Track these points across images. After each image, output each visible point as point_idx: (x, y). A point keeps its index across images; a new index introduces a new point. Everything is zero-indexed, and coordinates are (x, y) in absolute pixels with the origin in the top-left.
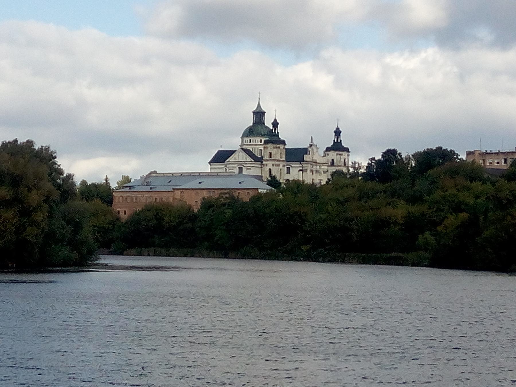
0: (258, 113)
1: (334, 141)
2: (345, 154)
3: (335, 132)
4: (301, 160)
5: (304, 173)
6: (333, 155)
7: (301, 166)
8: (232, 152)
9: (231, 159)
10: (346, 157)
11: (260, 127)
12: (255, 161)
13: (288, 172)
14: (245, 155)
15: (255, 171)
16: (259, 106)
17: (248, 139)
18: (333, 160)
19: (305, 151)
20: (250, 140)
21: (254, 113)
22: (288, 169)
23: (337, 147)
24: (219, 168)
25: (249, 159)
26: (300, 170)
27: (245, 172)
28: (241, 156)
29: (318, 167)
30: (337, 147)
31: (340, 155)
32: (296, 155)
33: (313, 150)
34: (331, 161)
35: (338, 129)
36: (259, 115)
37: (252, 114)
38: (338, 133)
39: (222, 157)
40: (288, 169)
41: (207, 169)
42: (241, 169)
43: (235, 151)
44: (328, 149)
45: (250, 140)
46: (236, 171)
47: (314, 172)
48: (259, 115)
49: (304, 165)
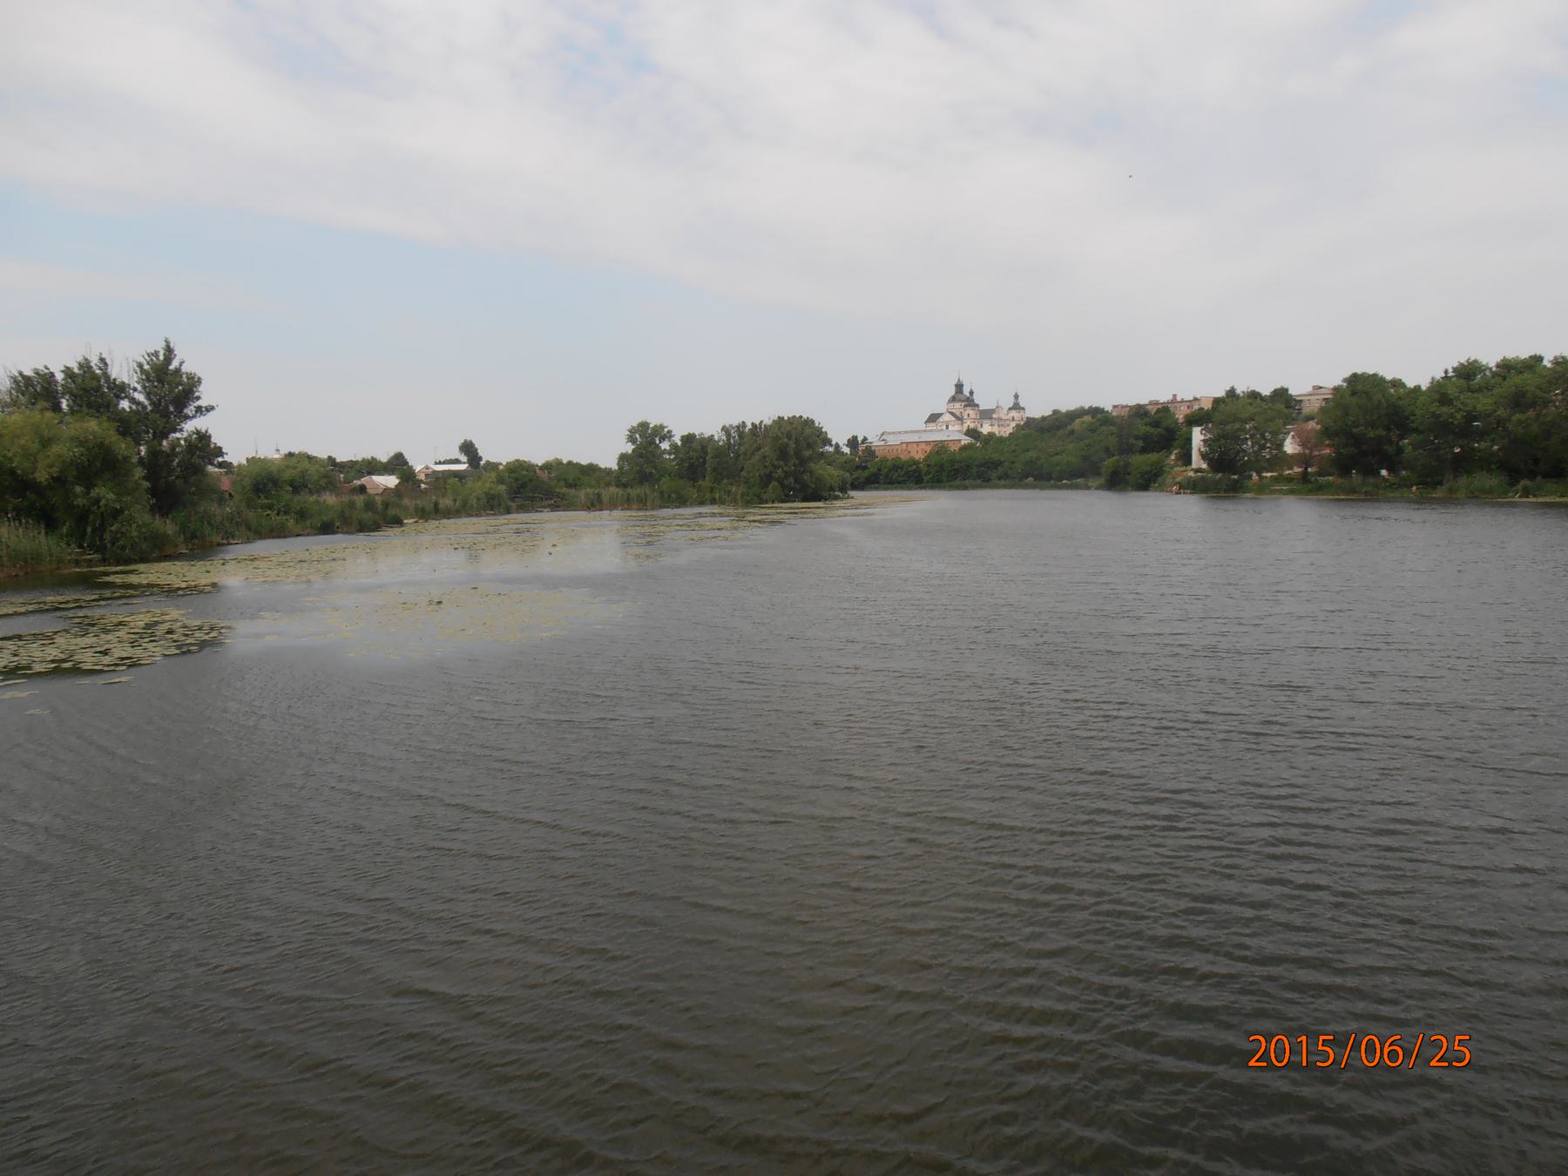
6: (1014, 413)
8: (940, 415)
11: (962, 396)
15: (957, 427)
19: (993, 411)
23: (1016, 407)
24: (932, 426)
28: (947, 417)
30: (1016, 407)
32: (987, 415)
36: (959, 387)
38: (1016, 397)
39: (933, 418)
41: (923, 427)
48: (959, 387)
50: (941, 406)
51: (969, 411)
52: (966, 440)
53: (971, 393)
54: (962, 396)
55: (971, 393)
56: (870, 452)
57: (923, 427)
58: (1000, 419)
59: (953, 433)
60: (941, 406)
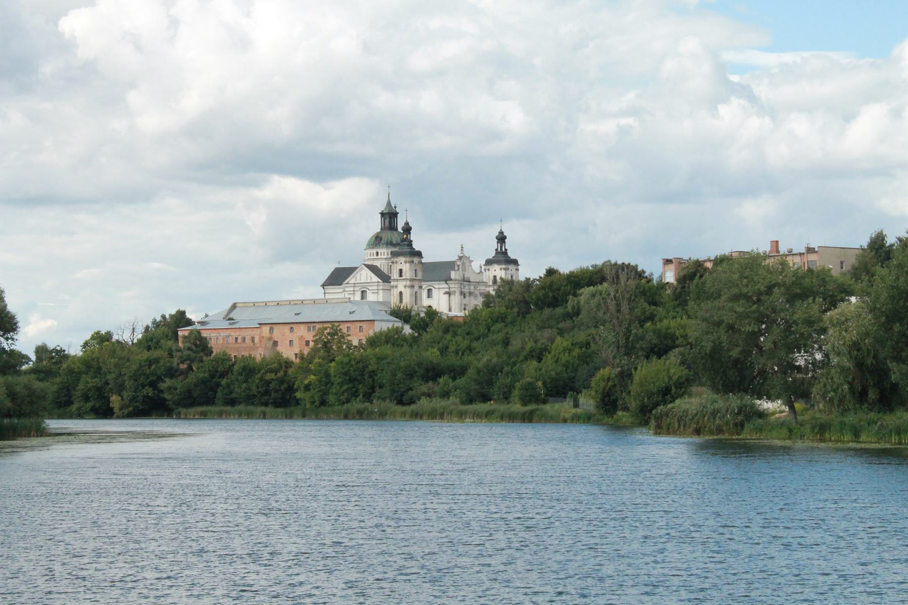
0: (389, 213)
1: (497, 250)
2: (512, 267)
3: (497, 238)
4: (448, 279)
5: (452, 297)
6: (498, 271)
7: (446, 286)
9: (351, 280)
10: (514, 272)
12: (384, 282)
13: (429, 295)
16: (389, 204)
17: (374, 251)
18: (495, 277)
19: (451, 265)
20: (377, 253)
21: (382, 214)
22: (429, 291)
23: (503, 258)
24: (335, 293)
25: (375, 279)
26: (446, 293)
27: (371, 297)
28: (364, 276)
29: (472, 287)
31: (505, 269)
33: (464, 264)
34: (492, 278)
35: (501, 233)
37: (380, 216)
38: (501, 239)
39: (339, 277)
40: (429, 291)
41: (317, 292)
42: (363, 293)
43: (356, 268)
44: (489, 262)
45: (377, 253)
46: (358, 297)
47: (467, 295)
49: (451, 286)
51: (403, 264)
52: (387, 324)
54: (394, 234)
55: (407, 229)
56: (200, 344)
57: (317, 292)
58: (465, 281)
59: (367, 307)
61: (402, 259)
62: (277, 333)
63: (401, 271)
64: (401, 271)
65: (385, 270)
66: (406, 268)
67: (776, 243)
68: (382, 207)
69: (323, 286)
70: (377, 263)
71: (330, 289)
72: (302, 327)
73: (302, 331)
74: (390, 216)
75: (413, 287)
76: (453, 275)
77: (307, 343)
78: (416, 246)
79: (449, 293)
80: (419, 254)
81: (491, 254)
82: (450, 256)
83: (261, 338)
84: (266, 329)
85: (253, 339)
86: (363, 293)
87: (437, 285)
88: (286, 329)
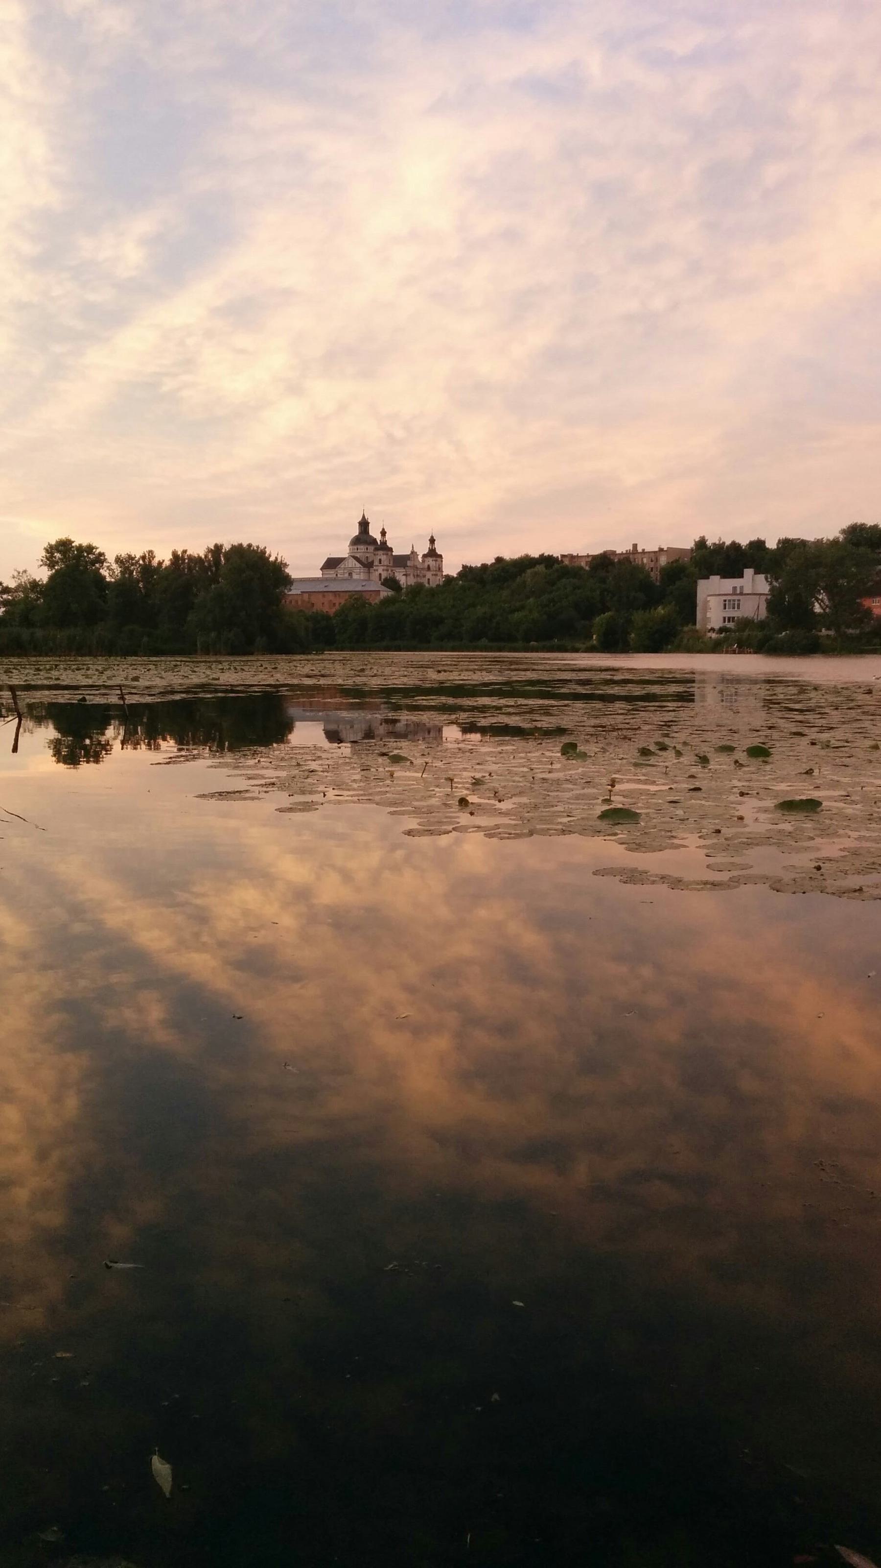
2: (439, 559)
4: (405, 566)
6: (430, 561)
9: (342, 566)
14: (355, 562)
16: (364, 517)
21: (360, 523)
23: (432, 553)
24: (331, 573)
25: (358, 565)
27: (355, 576)
28: (353, 563)
30: (432, 553)
32: (401, 561)
35: (432, 537)
38: (432, 541)
39: (332, 564)
41: (319, 574)
44: (424, 556)
46: (347, 575)
48: (364, 524)
50: (342, 550)
52: (386, 593)
53: (383, 533)
55: (383, 533)
58: (415, 567)
60: (342, 550)
61: (381, 552)
62: (313, 599)
63: (380, 560)
64: (380, 560)
65: (363, 560)
66: (383, 558)
67: (635, 546)
68: (360, 519)
69: (321, 569)
70: (358, 555)
71: (326, 571)
72: (330, 594)
73: (331, 597)
74: (364, 524)
75: (387, 570)
76: (409, 563)
77: (334, 604)
78: (389, 544)
79: (405, 575)
80: (391, 550)
81: (426, 552)
82: (408, 552)
83: (303, 601)
84: (306, 596)
85: (297, 602)
86: (350, 574)
87: (398, 569)
88: (320, 596)
